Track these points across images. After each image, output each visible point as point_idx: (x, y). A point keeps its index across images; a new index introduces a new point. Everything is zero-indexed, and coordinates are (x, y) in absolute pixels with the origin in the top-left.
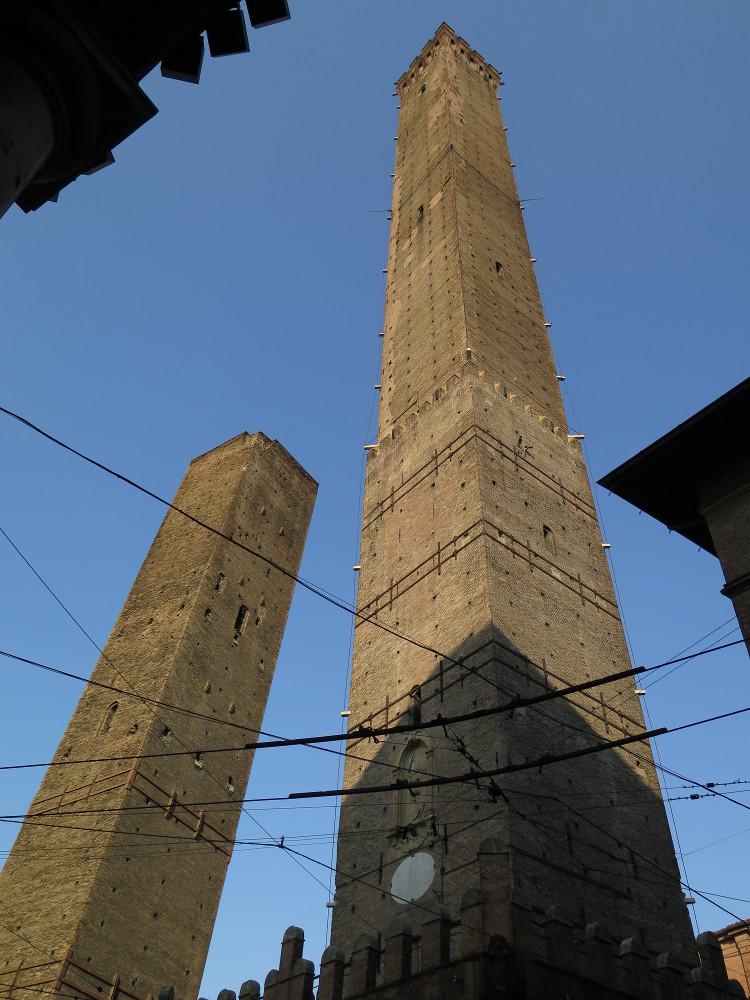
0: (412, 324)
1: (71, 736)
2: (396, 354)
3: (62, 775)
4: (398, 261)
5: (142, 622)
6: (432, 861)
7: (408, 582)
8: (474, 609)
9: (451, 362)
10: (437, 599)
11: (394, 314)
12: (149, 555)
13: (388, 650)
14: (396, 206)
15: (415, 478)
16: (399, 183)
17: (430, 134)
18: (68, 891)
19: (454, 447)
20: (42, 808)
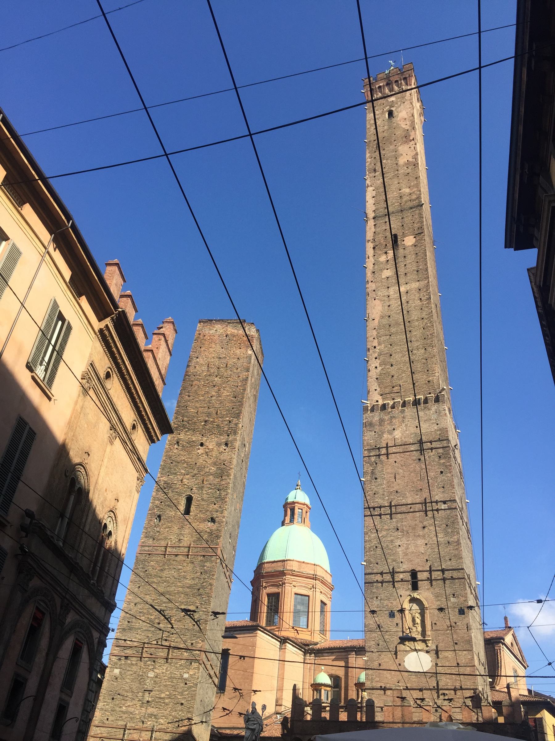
0: (393, 330)
1: (157, 507)
2: (379, 344)
3: (159, 532)
4: (376, 267)
5: (193, 441)
6: (430, 659)
7: (403, 509)
8: (451, 547)
9: (427, 382)
10: (426, 529)
11: (375, 309)
12: (184, 388)
13: (392, 541)
14: (371, 215)
15: (406, 446)
16: (370, 193)
17: (401, 171)
19: (434, 445)
20: (148, 551)
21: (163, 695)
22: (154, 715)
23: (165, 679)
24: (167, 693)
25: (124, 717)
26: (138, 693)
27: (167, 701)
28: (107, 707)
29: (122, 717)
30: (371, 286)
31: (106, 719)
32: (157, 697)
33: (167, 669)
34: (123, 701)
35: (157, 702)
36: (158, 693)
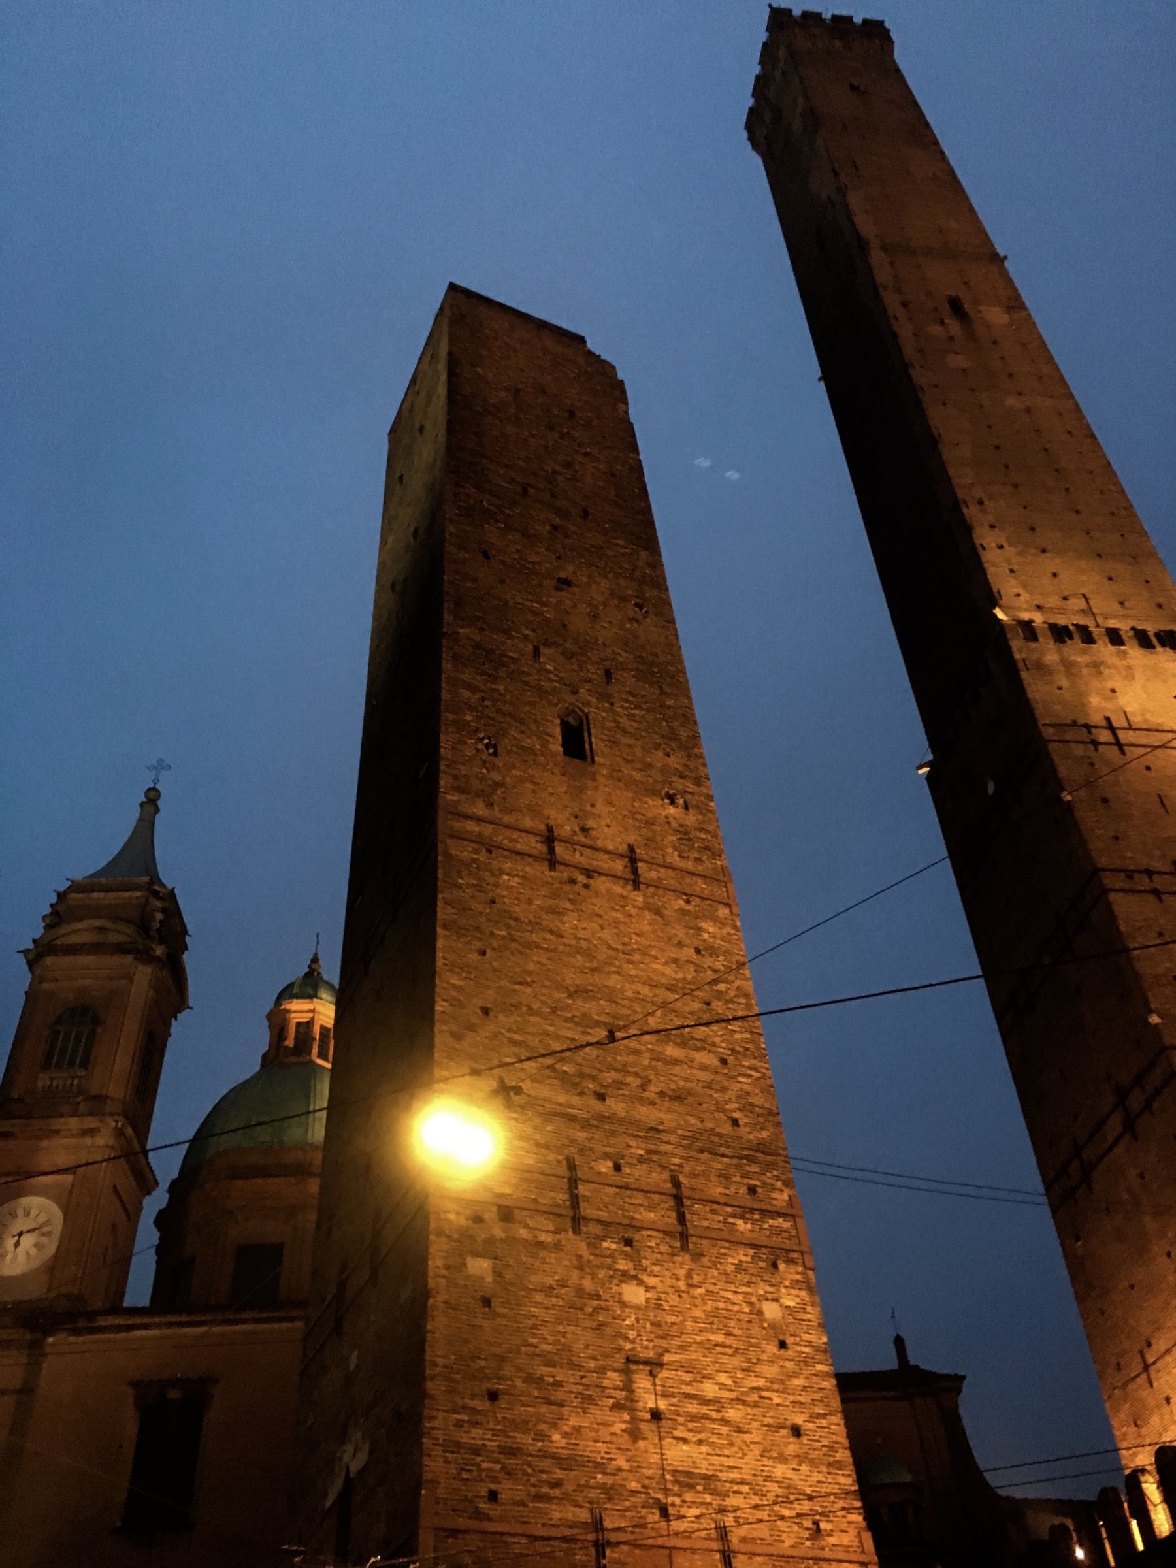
18: (704, 1068)
21: (709, 1390)
22: (706, 1477)
23: (695, 1320)
24: (723, 1378)
25: (570, 1487)
26: (601, 1371)
27: (733, 1414)
28: (476, 1432)
29: (557, 1484)
30: (920, 376)
31: (484, 1493)
32: (688, 1396)
33: (689, 1276)
34: (543, 1409)
35: (694, 1418)
36: (688, 1377)
